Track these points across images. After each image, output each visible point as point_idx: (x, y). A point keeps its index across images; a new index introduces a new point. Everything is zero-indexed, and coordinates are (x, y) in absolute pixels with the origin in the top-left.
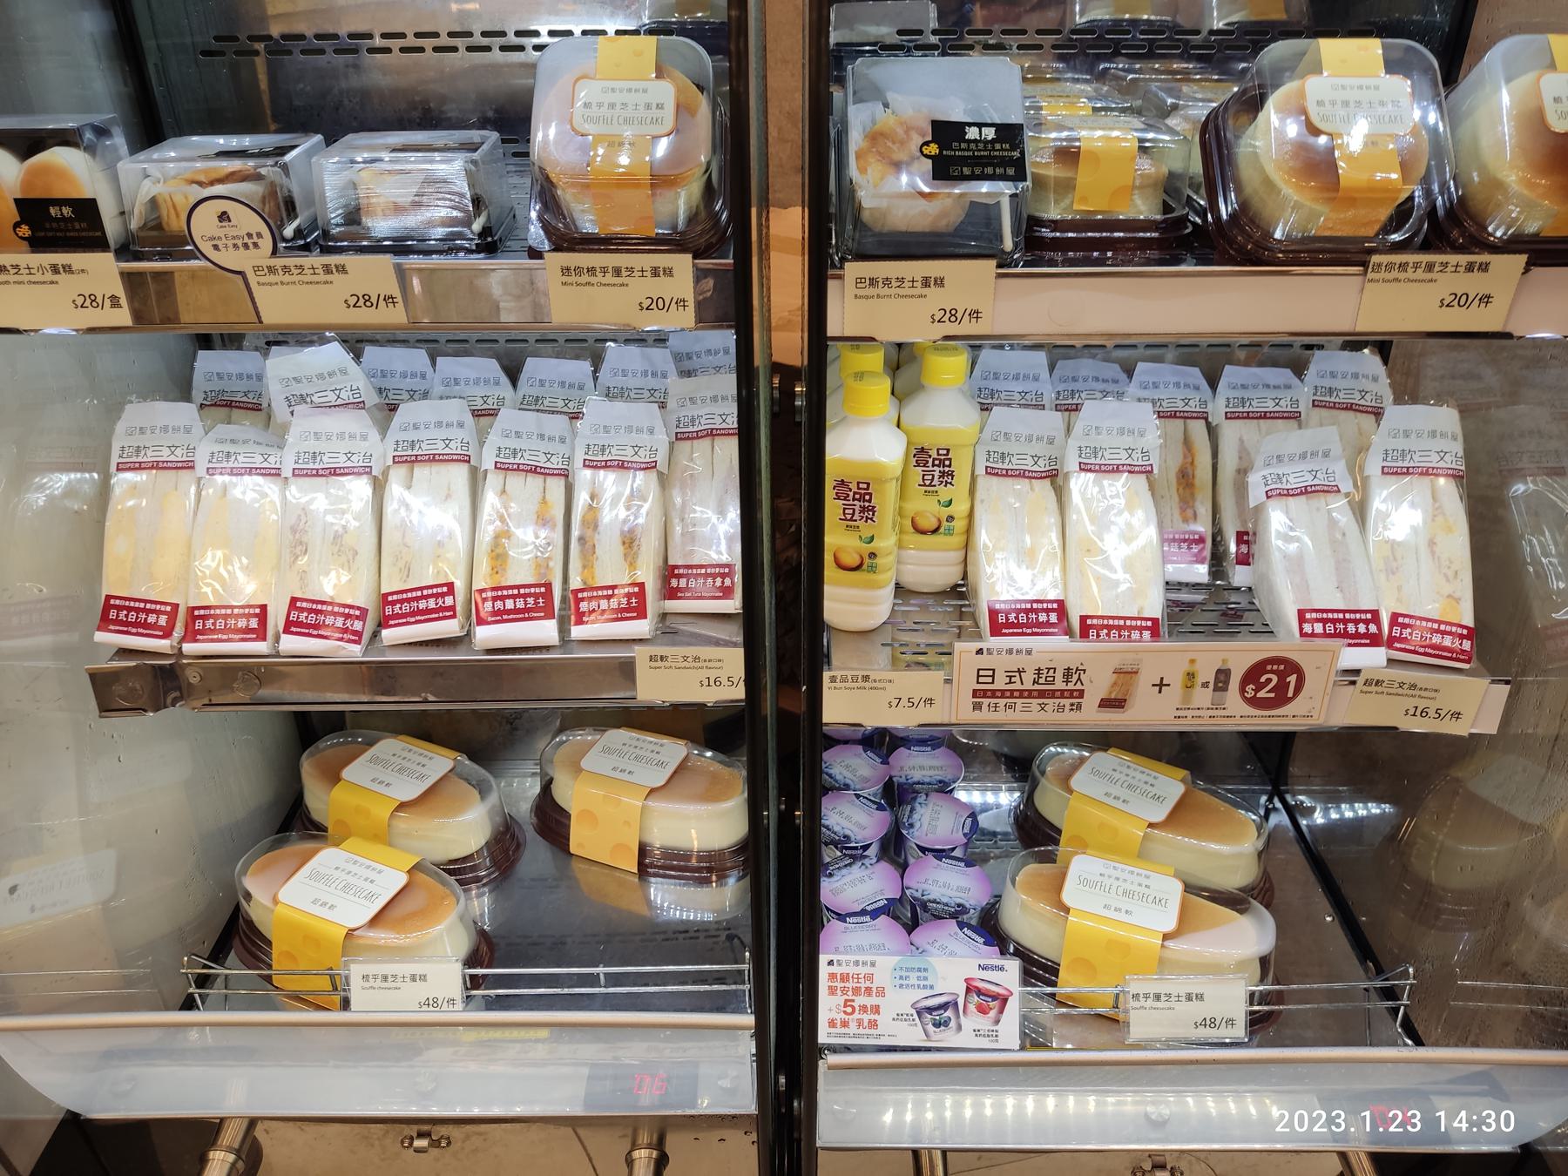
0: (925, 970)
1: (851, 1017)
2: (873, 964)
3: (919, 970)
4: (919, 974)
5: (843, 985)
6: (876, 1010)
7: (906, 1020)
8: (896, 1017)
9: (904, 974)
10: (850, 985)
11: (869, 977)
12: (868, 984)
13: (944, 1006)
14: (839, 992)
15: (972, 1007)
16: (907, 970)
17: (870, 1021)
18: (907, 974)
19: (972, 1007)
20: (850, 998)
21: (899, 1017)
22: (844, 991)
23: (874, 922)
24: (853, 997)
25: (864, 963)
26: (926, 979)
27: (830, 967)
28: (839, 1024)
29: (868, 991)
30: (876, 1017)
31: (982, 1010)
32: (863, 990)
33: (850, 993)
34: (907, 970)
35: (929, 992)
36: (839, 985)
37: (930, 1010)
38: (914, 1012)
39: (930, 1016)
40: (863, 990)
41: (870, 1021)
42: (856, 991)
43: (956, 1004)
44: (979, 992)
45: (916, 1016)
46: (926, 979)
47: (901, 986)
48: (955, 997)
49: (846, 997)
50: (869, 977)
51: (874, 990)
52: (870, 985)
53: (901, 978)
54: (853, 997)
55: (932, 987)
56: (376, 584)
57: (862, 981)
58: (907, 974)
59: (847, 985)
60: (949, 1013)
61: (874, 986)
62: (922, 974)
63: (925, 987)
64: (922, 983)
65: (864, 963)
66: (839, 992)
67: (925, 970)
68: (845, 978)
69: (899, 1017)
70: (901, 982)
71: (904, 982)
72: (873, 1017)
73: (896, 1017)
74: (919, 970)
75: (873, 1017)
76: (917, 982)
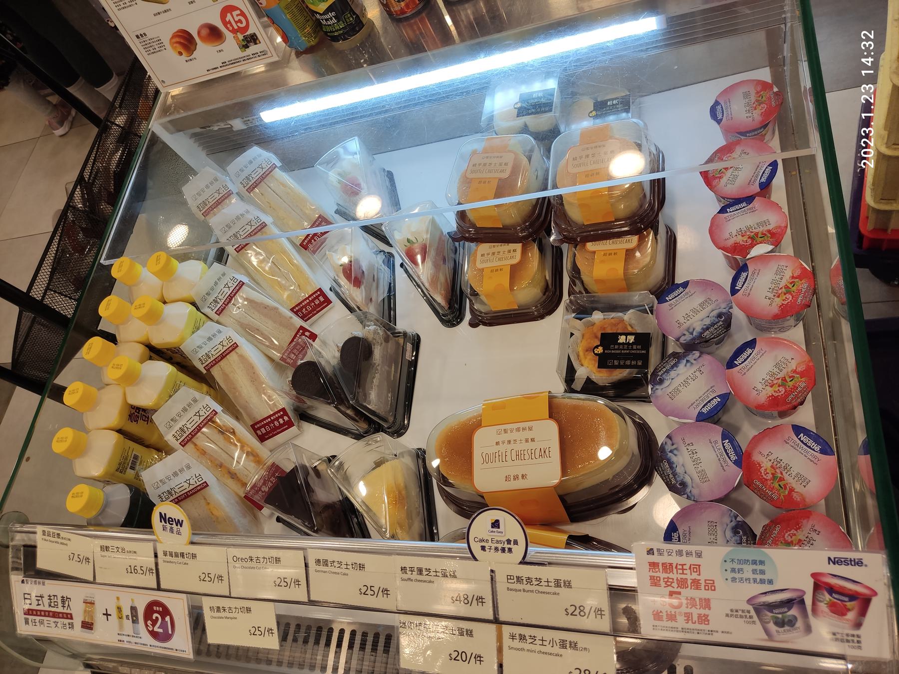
0: (762, 563)
1: (677, 611)
2: (699, 555)
3: (754, 562)
4: (755, 567)
5: (666, 575)
6: (707, 603)
7: (741, 617)
8: (729, 613)
9: (737, 566)
10: (674, 576)
11: (696, 568)
12: (695, 576)
13: (789, 603)
14: (662, 583)
15: (823, 607)
16: (740, 562)
17: (700, 616)
18: (740, 566)
19: (823, 607)
20: (675, 590)
21: (733, 613)
22: (668, 582)
23: (818, 455)
24: (679, 590)
25: (689, 554)
26: (762, 572)
27: (650, 556)
28: (665, 617)
29: (696, 584)
30: (706, 612)
31: (838, 610)
32: (689, 582)
33: (675, 585)
34: (740, 562)
35: (767, 588)
36: (663, 575)
37: (771, 607)
38: (750, 608)
39: (770, 614)
40: (689, 582)
41: (700, 616)
42: (682, 583)
43: (802, 602)
44: (831, 590)
45: (753, 613)
46: (762, 572)
47: (734, 580)
48: (798, 594)
49: (670, 589)
50: (696, 568)
51: (702, 582)
52: (698, 578)
53: (733, 570)
54: (679, 590)
55: (770, 582)
56: (259, 352)
57: (688, 572)
58: (740, 566)
59: (671, 576)
60: (794, 612)
61: (702, 578)
62: (759, 567)
63: (762, 581)
64: (758, 577)
65: (689, 554)
66: (662, 583)
67: (762, 563)
68: (668, 567)
69: (733, 613)
70: (733, 575)
71: (737, 575)
72: (703, 612)
73: (729, 613)
74: (754, 562)
75: (703, 612)
76: (752, 576)
